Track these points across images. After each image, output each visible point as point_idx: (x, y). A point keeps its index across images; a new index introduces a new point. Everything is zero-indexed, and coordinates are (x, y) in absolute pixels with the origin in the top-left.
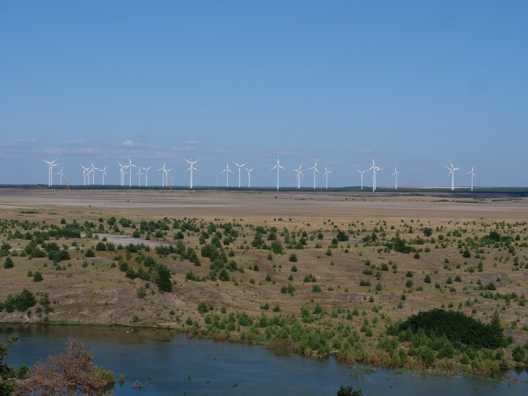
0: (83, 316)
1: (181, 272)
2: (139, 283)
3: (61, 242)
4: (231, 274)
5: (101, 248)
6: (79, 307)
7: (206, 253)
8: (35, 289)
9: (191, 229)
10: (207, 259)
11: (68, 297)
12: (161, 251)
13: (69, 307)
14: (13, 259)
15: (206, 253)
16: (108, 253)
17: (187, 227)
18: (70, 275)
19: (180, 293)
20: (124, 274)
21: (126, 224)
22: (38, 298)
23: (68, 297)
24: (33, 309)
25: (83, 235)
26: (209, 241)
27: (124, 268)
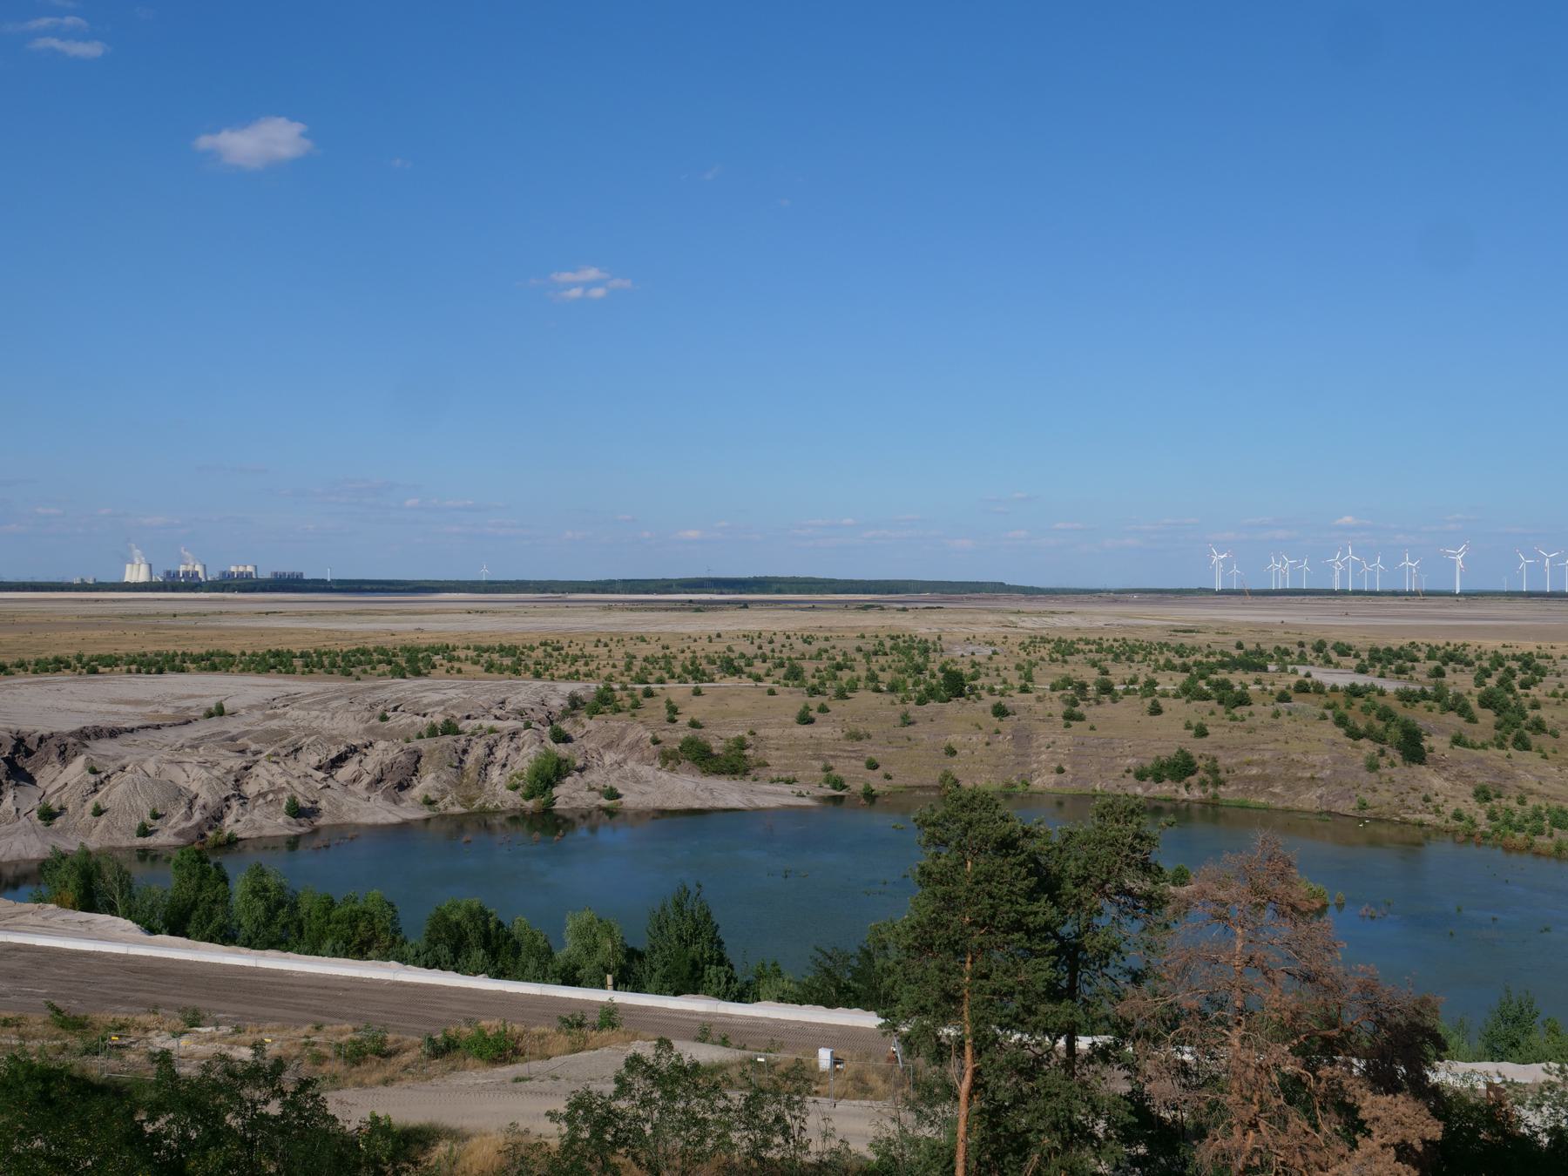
0: (1274, 795)
1: (1442, 731)
2: (1368, 747)
3: (1237, 678)
4: (1535, 740)
5: (1302, 688)
6: (1268, 781)
7: (1486, 701)
8: (1196, 748)
9: (1459, 662)
10: (1490, 713)
11: (1249, 764)
12: (1406, 697)
13: (1251, 779)
14: (1162, 701)
15: (1486, 701)
16: (1313, 697)
17: (1450, 657)
18: (1251, 730)
19: (1440, 766)
20: (1342, 731)
21: (1344, 650)
22: (1201, 763)
23: (1249, 764)
24: (1193, 779)
25: (1272, 667)
26: (1491, 682)
27: (1341, 721)
